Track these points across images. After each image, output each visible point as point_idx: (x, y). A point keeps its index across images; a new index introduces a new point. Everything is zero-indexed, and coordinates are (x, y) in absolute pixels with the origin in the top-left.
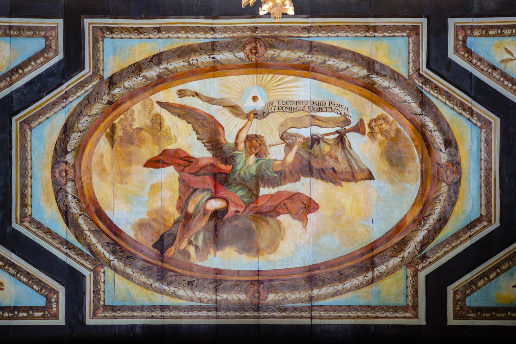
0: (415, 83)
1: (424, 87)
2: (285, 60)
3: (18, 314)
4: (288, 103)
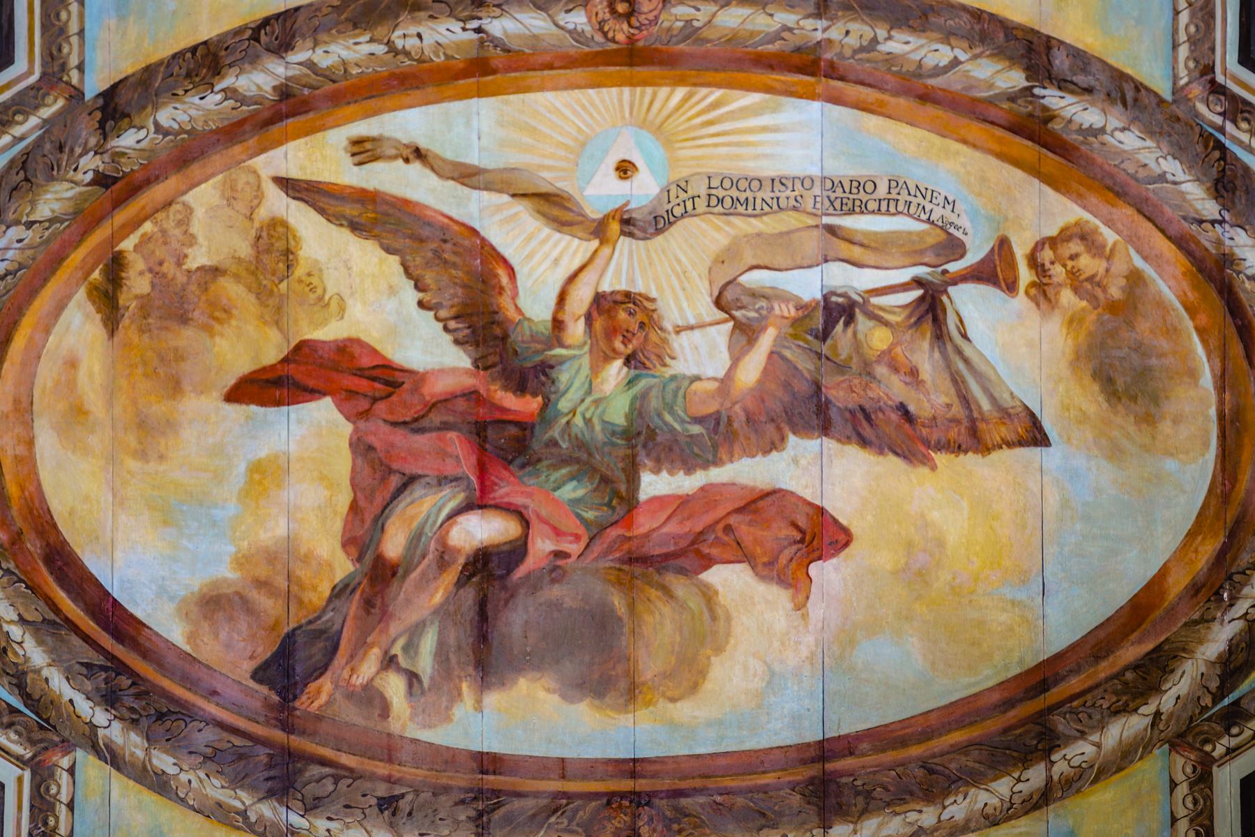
0: (1197, 115)
1: (1229, 127)
2: (733, 38)
4: (743, 185)
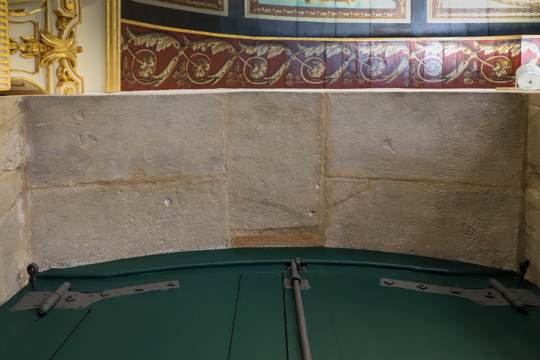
3: (375, 15)
